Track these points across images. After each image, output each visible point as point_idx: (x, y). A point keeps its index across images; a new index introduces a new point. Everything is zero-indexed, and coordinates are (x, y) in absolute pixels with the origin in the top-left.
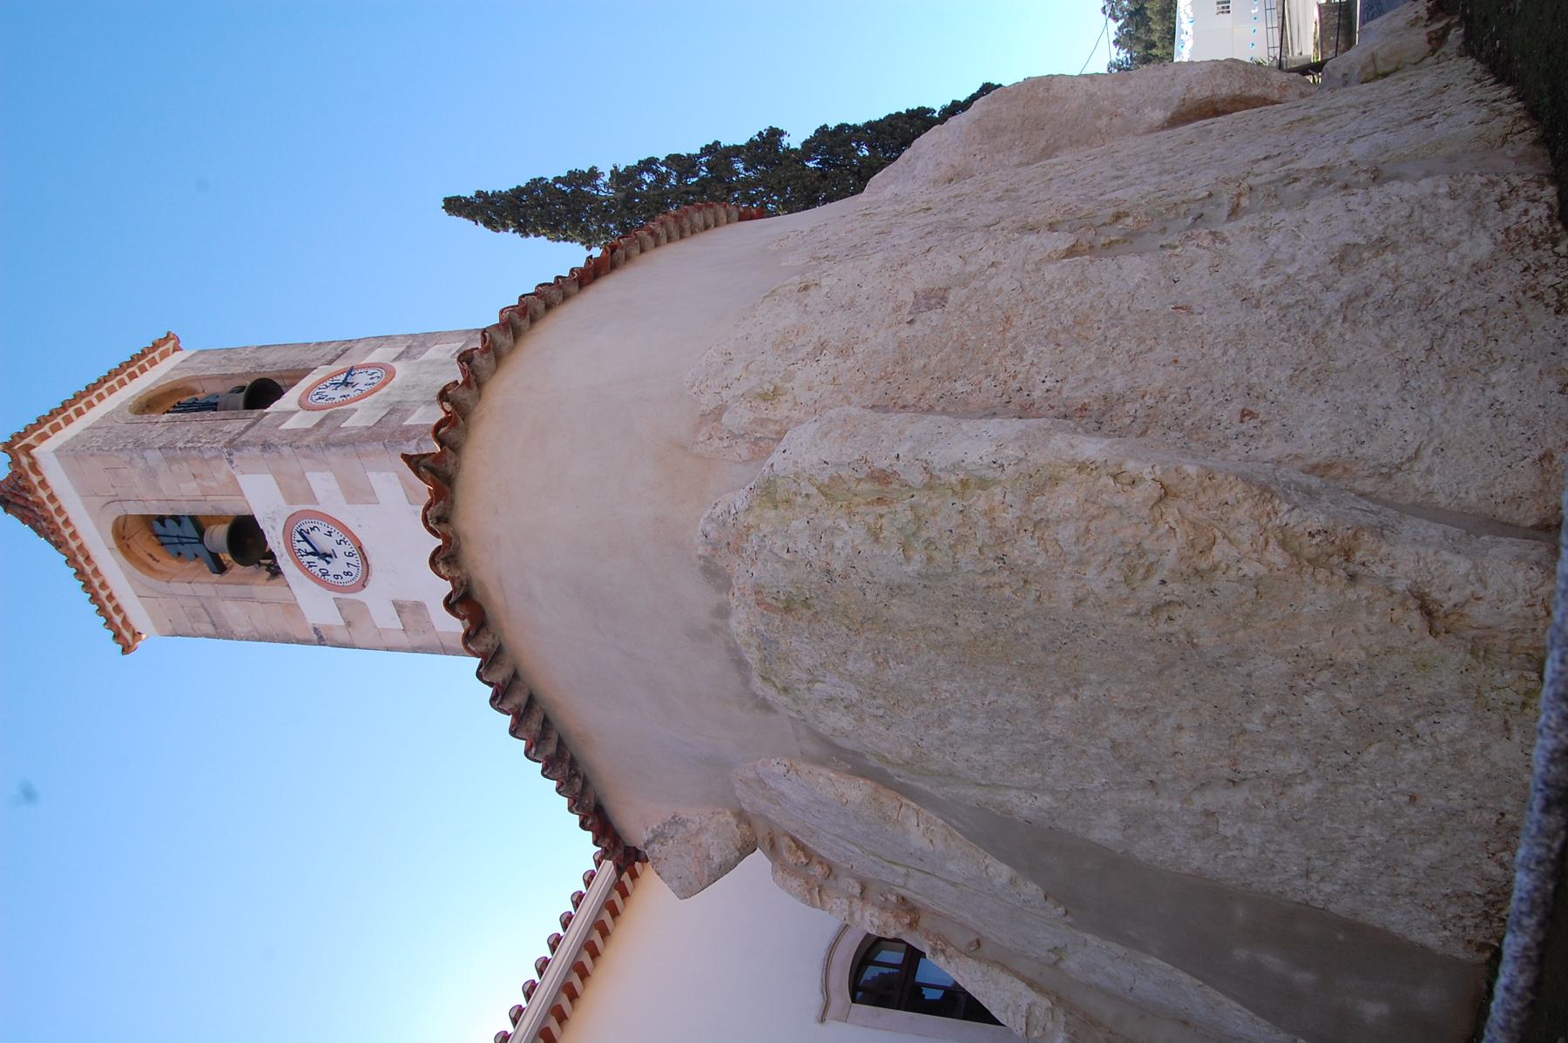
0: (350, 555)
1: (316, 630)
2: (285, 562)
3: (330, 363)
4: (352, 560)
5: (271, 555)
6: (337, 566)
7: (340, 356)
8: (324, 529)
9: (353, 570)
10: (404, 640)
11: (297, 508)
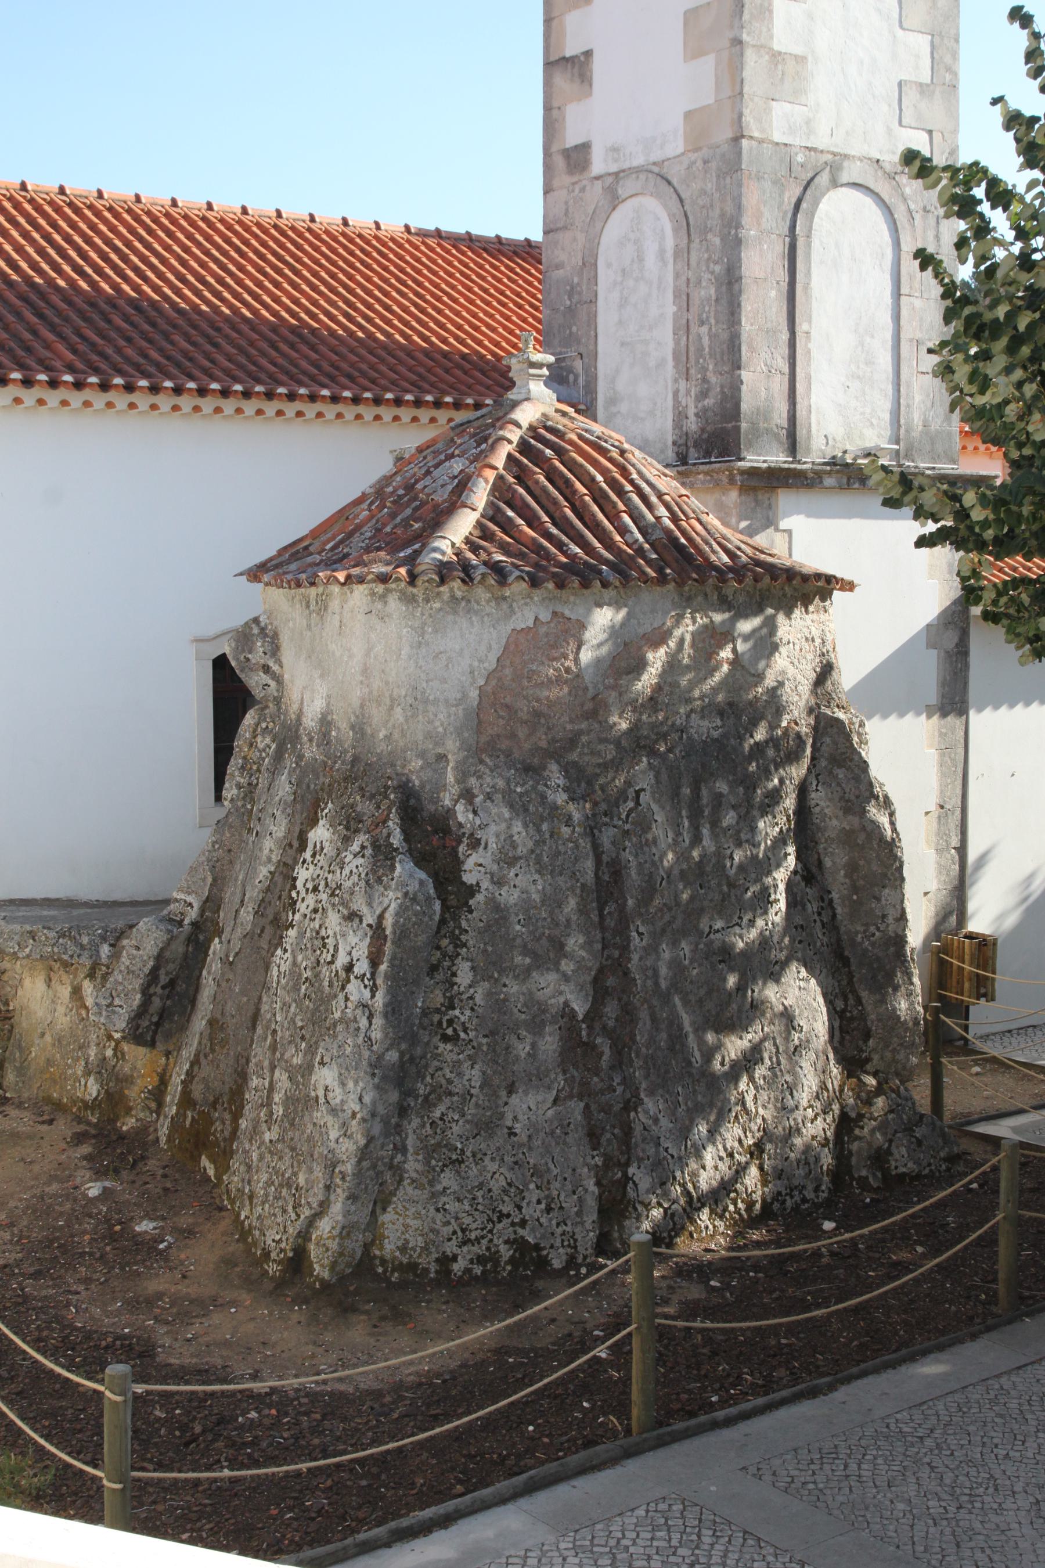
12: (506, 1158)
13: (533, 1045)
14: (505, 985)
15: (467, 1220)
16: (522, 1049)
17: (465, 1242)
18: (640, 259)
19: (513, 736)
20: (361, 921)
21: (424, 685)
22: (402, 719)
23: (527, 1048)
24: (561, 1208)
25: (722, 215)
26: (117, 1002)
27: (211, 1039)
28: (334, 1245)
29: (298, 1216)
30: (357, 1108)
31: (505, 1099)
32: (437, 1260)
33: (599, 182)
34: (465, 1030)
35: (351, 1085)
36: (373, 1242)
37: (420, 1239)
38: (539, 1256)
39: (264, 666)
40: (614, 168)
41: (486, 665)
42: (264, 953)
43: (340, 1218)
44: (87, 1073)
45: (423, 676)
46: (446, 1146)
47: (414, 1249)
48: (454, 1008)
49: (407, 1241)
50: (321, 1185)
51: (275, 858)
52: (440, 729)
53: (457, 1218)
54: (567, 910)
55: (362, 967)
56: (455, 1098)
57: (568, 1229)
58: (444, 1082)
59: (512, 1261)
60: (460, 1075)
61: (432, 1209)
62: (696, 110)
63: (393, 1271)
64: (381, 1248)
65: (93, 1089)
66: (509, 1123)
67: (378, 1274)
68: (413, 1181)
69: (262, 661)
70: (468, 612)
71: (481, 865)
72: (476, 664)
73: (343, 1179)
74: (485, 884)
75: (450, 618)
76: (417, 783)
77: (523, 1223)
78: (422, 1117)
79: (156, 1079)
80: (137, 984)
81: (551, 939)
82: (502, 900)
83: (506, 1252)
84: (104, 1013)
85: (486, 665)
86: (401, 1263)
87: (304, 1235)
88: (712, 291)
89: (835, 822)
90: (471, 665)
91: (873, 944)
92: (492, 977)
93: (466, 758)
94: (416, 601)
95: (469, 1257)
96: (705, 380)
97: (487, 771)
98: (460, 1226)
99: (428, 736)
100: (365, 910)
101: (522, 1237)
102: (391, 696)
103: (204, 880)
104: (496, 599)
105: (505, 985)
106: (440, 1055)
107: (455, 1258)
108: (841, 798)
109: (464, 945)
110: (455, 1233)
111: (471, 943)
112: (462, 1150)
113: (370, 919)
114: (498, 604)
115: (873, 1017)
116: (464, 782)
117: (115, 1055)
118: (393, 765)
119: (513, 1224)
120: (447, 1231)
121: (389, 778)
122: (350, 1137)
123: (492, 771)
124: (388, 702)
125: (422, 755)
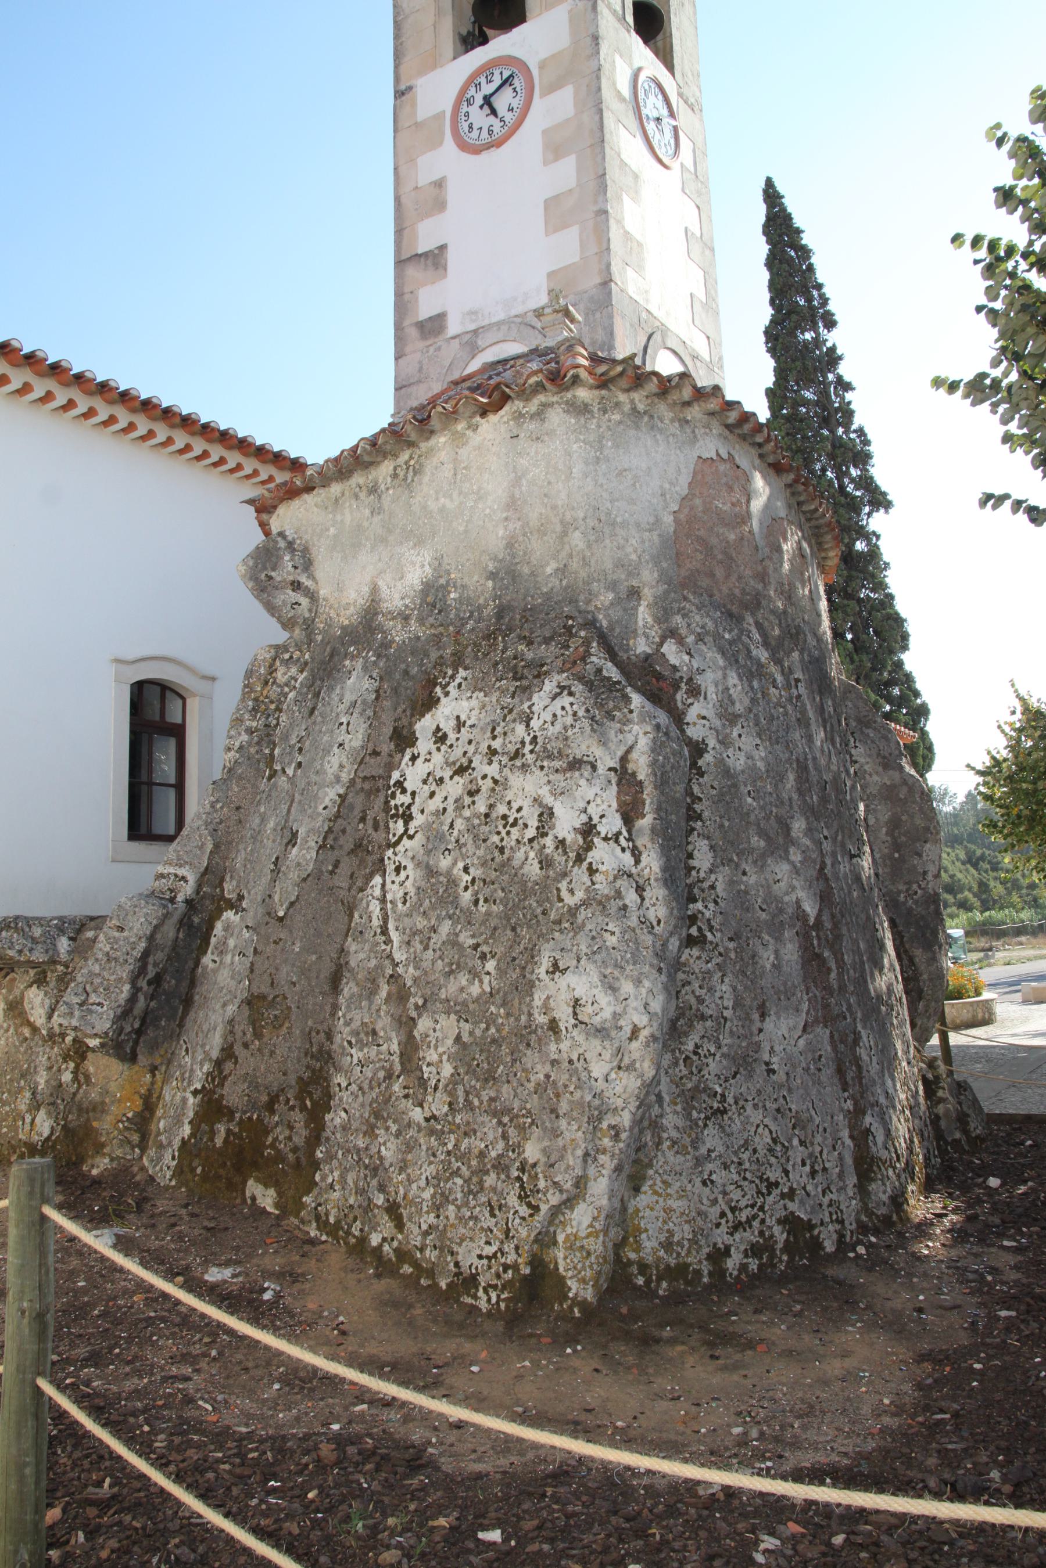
0: (490, 132)
1: (410, 88)
2: (480, 55)
3: (680, 95)
4: (485, 134)
5: (484, 40)
6: (479, 117)
7: (686, 102)
8: (515, 103)
9: (475, 134)
10: (407, 188)
11: (535, 72)
12: (768, 1104)
13: (776, 952)
14: (744, 873)
15: (736, 1195)
16: (767, 958)
17: (737, 1227)
19: (712, 575)
20: (594, 768)
21: (609, 505)
22: (581, 545)
23: (772, 958)
24: (825, 1169)
26: (93, 998)
27: (253, 1022)
28: (596, 1245)
29: (536, 1209)
30: (641, 1020)
31: (758, 1024)
32: (709, 1257)
33: (457, 341)
34: (711, 929)
35: (627, 987)
36: (625, 1239)
37: (686, 1227)
38: (812, 1236)
39: (293, 583)
40: (472, 327)
41: (678, 489)
42: (342, 893)
43: (604, 1202)
44: (35, 1106)
45: (605, 495)
46: (705, 1090)
47: (679, 1243)
48: (694, 900)
49: (671, 1233)
50: (579, 1153)
51: (345, 777)
52: (634, 557)
53: (725, 1193)
54: (788, 786)
55: (613, 823)
56: (709, 1023)
57: (834, 1197)
58: (693, 1001)
59: (787, 1247)
60: (711, 990)
61: (698, 1182)
63: (660, 1279)
64: (638, 1249)
65: (44, 1125)
66: (766, 1057)
67: (637, 1288)
68: (674, 1143)
69: (291, 578)
70: (652, 428)
71: (704, 718)
72: (667, 486)
73: (616, 1137)
74: (712, 742)
75: (632, 432)
76: (605, 623)
77: (791, 1195)
78: (673, 1051)
79: (139, 1102)
80: (124, 972)
81: (780, 820)
82: (730, 762)
83: (780, 1236)
84: (77, 1013)
85: (678, 489)
86: (668, 1266)
87: (545, 1240)
89: (875, 778)
90: (661, 487)
91: (916, 902)
92: (731, 860)
93: (667, 593)
94: (590, 412)
95: (742, 1248)
97: (693, 608)
98: (728, 1203)
99: (619, 564)
100: (598, 751)
101: (792, 1213)
102: (562, 522)
103: (201, 847)
104: (679, 420)
105: (744, 873)
106: (685, 965)
107: (727, 1252)
108: (879, 755)
109: (699, 817)
110: (723, 1214)
111: (706, 814)
112: (723, 1096)
113: (606, 761)
114: (681, 426)
115: (925, 977)
116: (666, 620)
117: (76, 1079)
118: (573, 601)
119: (783, 1196)
120: (714, 1212)
121: (569, 617)
122: (630, 1068)
123: (699, 609)
124: (559, 528)
125: (613, 586)
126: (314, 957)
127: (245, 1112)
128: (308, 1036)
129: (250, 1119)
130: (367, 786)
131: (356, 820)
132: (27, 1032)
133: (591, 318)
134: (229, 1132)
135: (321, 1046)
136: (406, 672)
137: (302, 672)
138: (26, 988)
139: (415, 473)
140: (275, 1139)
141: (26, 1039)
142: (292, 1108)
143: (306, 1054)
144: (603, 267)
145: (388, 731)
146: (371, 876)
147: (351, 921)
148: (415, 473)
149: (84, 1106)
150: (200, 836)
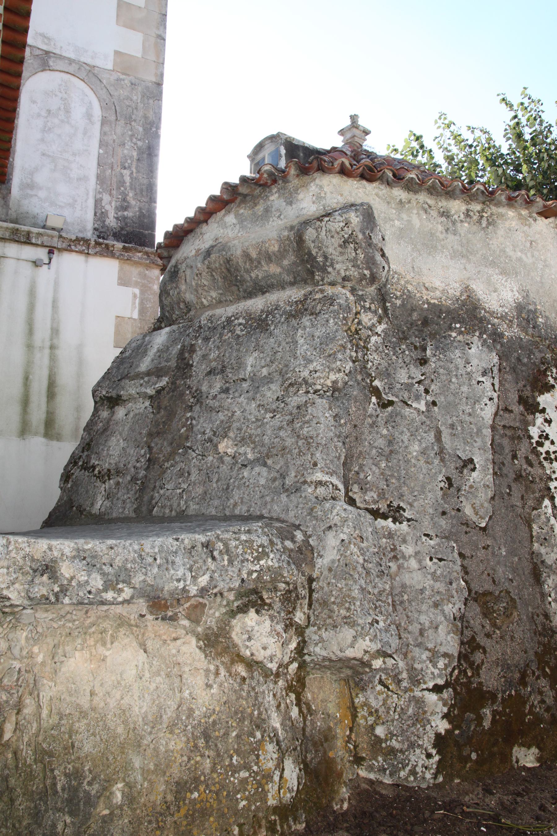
18: (68, 111)
25: (146, 117)
42: (520, 511)
62: (126, 54)
88: (135, 154)
96: (124, 200)
103: (339, 458)
126: (516, 559)
127: (504, 692)
128: (532, 619)
129: (510, 695)
130: (509, 433)
131: (509, 457)
132: (241, 669)
133: (146, 101)
134: (494, 713)
135: (543, 625)
136: (519, 360)
137: (380, 323)
138: (233, 614)
139: (489, 224)
140: (532, 706)
141: (244, 679)
142: (538, 678)
143: (535, 633)
144: (159, 73)
145: (514, 397)
146: (540, 501)
147: (531, 531)
148: (489, 224)
149: (316, 738)
150: (336, 447)
